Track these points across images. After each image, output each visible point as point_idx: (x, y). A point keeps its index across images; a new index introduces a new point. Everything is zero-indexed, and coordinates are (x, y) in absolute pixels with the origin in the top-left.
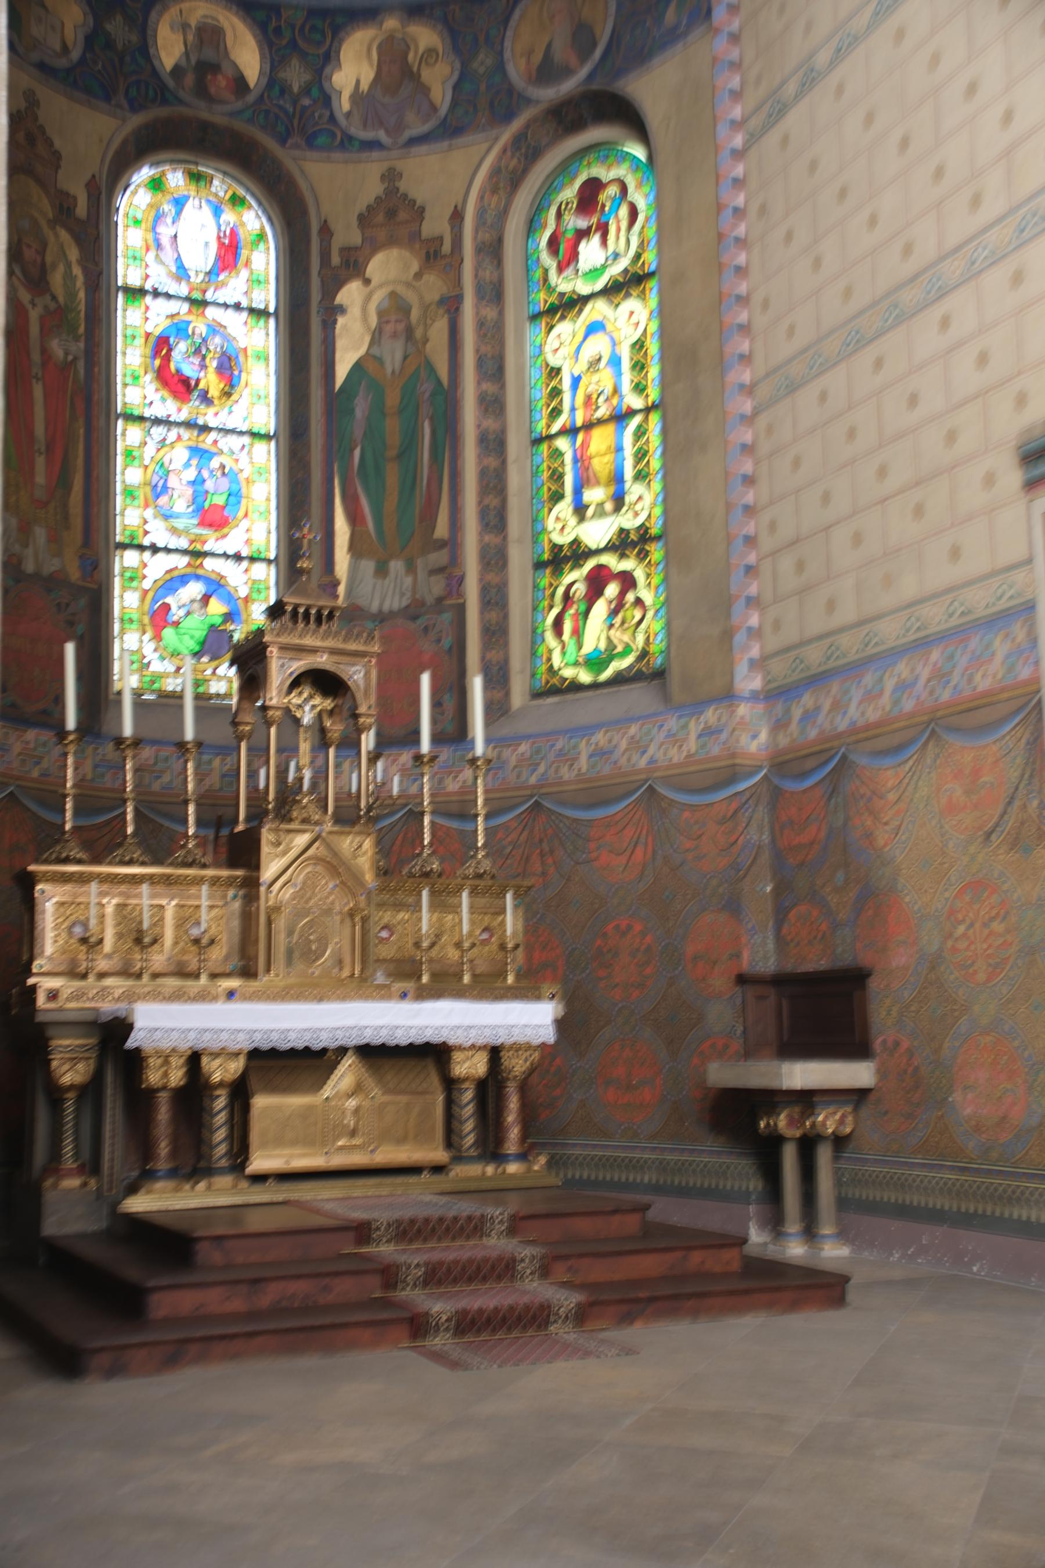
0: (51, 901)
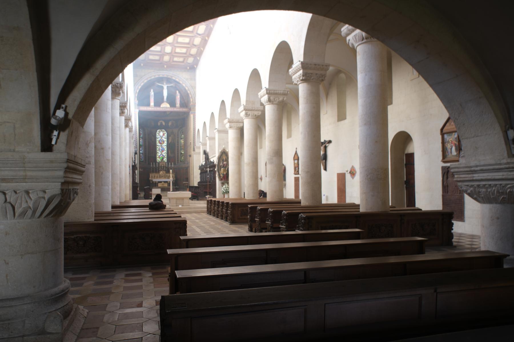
0: (151, 175)
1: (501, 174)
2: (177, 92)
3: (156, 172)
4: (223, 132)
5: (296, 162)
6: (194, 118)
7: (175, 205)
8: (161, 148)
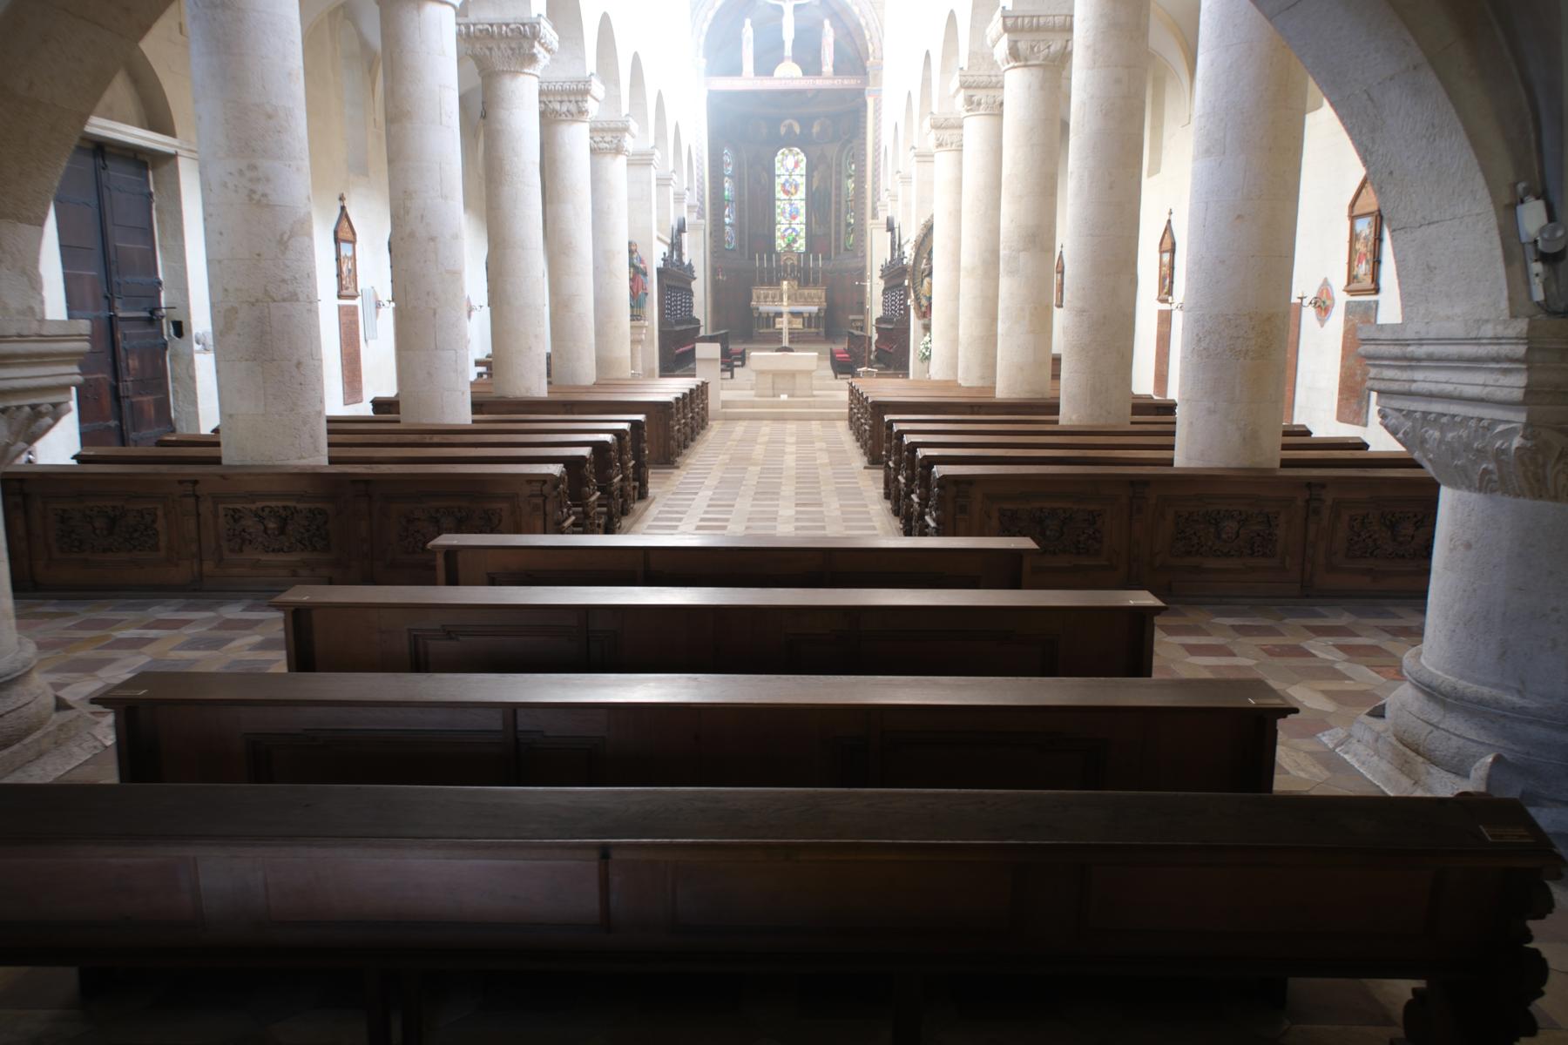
1: (1480, 378)
2: (827, 23)
3: (770, 283)
4: (925, 158)
5: (1166, 257)
6: (877, 111)
7: (770, 392)
8: (788, 208)
